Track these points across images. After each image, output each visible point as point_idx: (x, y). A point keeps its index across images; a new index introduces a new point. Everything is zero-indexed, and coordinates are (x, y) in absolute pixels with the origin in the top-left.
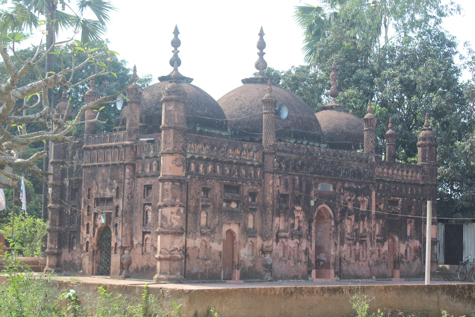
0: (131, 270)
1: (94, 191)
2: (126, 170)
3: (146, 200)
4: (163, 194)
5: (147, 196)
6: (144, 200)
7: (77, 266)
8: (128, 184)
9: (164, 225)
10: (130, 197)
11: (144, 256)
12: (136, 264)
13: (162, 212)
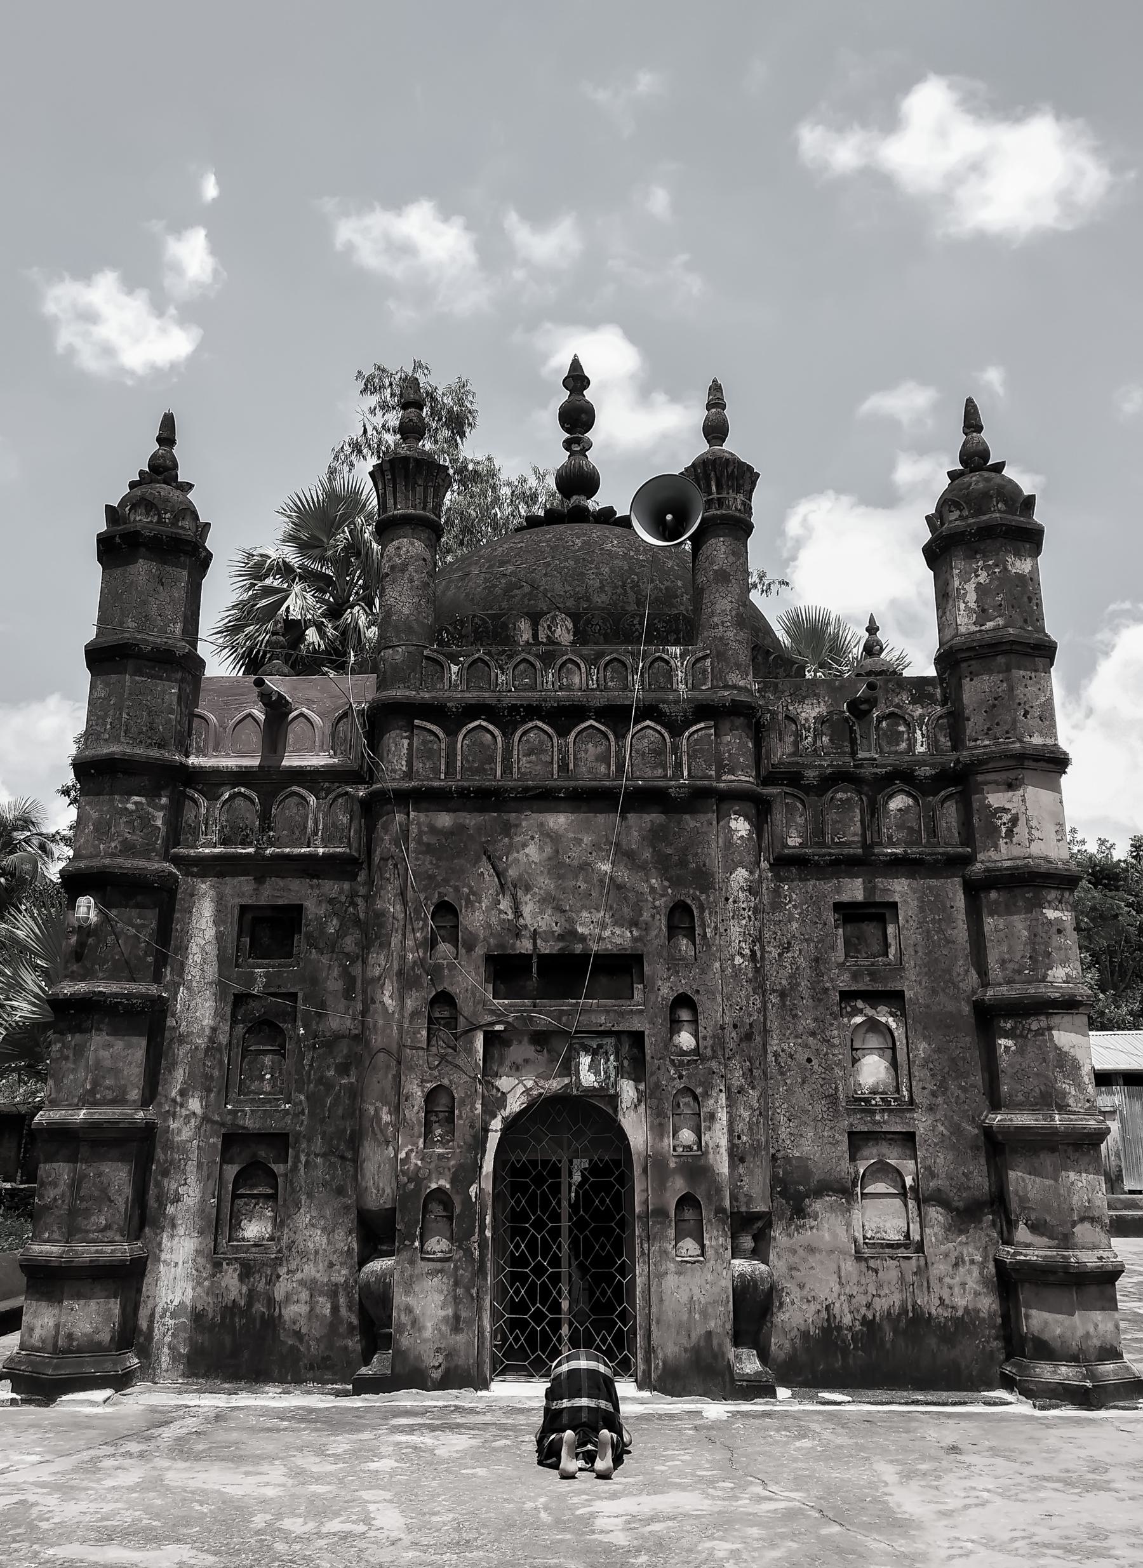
0: (779, 1345)
1: (475, 920)
3: (855, 977)
4: (1047, 944)
6: (846, 976)
7: (298, 1334)
9: (1071, 1101)
10: (758, 954)
11: (872, 1263)
12: (813, 1307)
13: (1054, 1032)
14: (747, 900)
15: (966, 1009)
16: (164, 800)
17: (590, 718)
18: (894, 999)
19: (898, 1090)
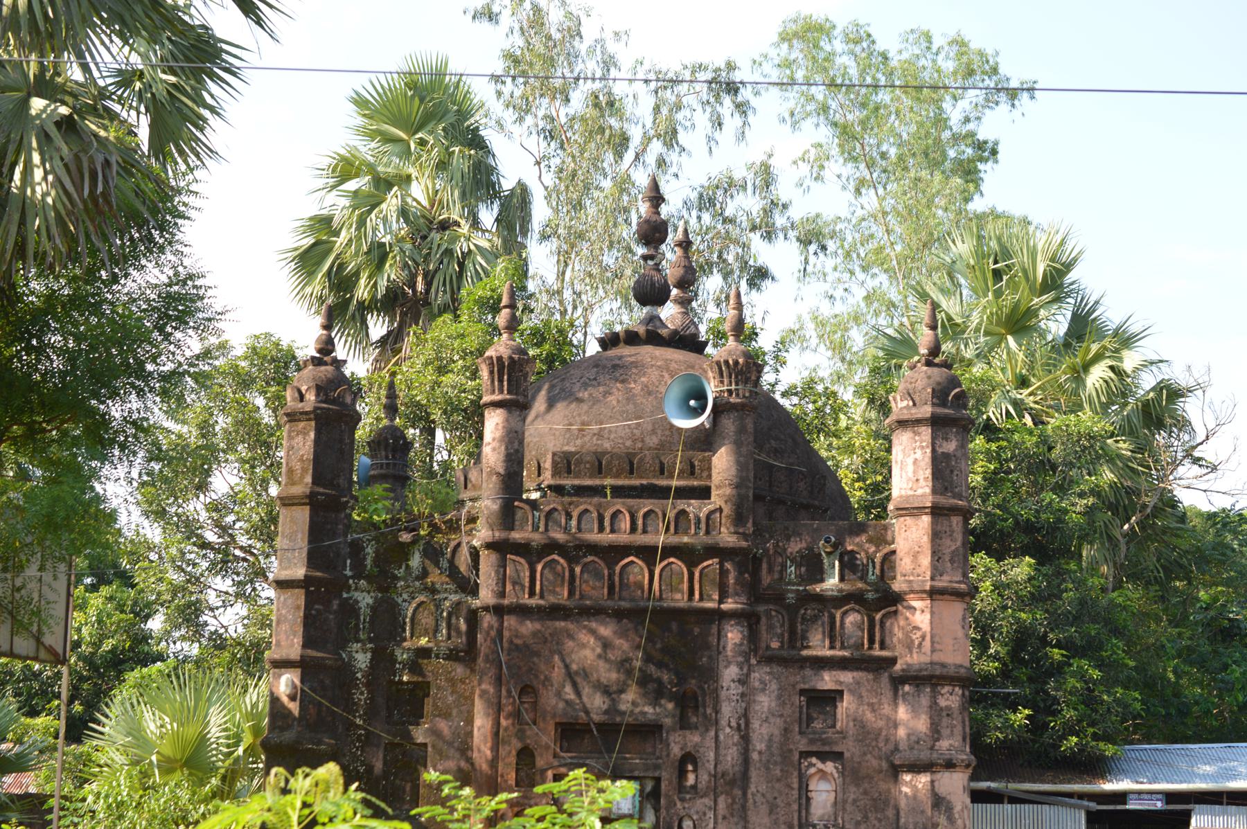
1: (550, 700)
2: (730, 635)
3: (812, 742)
5: (808, 726)
6: (804, 741)
8: (739, 681)
10: (743, 726)
13: (936, 784)
14: (736, 688)
15: (885, 765)
16: (335, 607)
17: (632, 555)
18: (837, 756)
19: (836, 819)
